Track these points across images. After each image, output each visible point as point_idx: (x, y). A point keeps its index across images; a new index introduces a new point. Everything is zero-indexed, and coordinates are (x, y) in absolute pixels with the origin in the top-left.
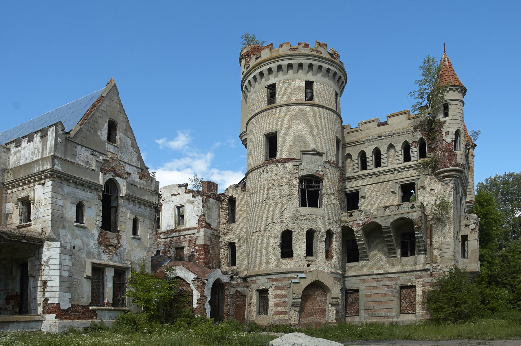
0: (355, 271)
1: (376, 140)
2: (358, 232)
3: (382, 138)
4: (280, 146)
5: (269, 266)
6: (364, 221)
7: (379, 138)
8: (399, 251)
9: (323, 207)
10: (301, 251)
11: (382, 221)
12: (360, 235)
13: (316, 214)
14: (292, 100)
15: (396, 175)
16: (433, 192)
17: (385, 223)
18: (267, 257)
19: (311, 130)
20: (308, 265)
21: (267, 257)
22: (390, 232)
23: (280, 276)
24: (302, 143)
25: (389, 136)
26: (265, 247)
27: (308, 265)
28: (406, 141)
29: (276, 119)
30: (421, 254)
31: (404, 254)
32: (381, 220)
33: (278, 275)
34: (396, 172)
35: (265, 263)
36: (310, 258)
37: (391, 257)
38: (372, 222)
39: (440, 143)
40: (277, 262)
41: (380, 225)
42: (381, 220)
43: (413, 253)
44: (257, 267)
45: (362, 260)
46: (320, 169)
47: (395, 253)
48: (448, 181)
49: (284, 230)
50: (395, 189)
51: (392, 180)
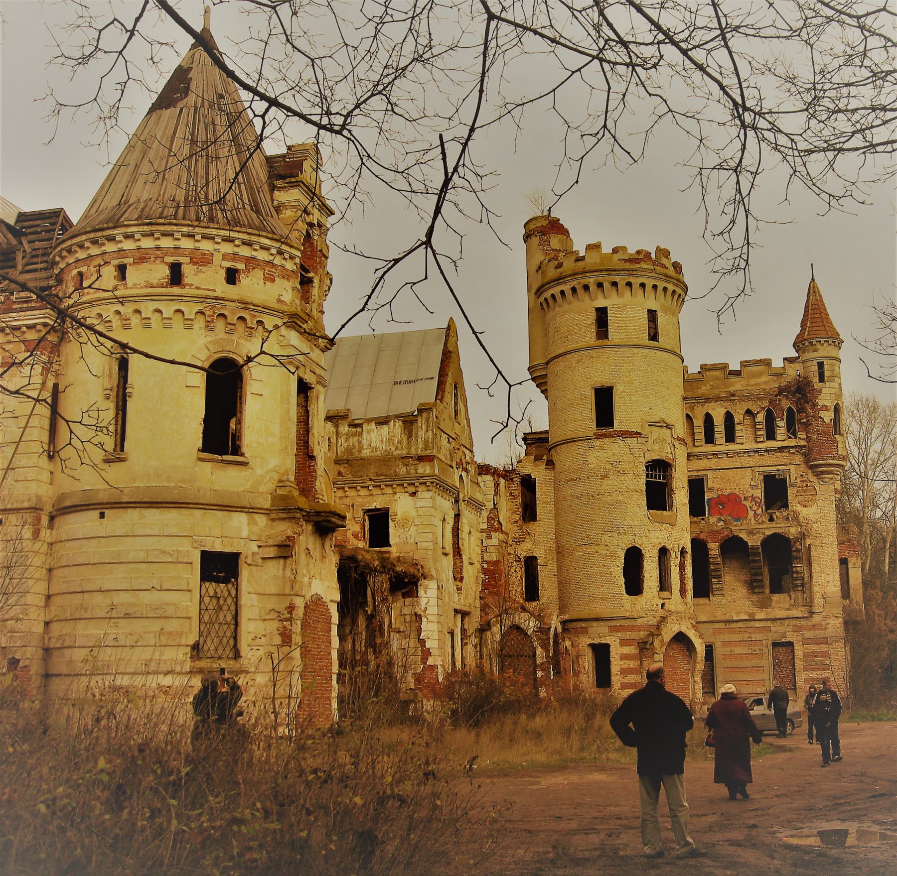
8: (767, 583)
17: (754, 541)
18: (604, 590)
20: (663, 605)
21: (604, 590)
27: (663, 605)
35: (602, 599)
36: (665, 594)
37: (755, 593)
41: (746, 543)
45: (713, 595)
47: (763, 587)
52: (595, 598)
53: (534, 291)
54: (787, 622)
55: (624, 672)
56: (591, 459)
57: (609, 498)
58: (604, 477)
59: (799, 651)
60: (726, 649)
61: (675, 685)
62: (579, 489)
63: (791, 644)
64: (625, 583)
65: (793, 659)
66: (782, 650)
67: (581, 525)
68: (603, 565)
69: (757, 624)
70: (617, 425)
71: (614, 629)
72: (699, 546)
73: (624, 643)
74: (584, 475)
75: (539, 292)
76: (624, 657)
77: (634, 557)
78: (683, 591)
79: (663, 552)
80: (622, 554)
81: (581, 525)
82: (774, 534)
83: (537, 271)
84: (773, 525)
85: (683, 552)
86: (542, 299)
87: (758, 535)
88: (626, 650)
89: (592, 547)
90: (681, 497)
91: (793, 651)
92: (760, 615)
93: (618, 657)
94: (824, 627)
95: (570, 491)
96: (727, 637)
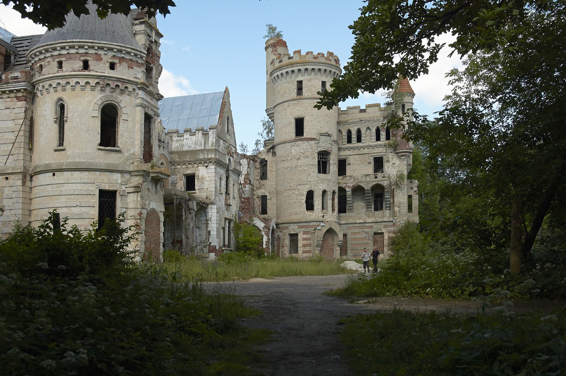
0: (344, 220)
2: (349, 191)
5: (298, 216)
6: (353, 184)
8: (373, 206)
9: (331, 173)
10: (319, 206)
13: (328, 179)
17: (367, 187)
19: (325, 117)
20: (323, 216)
22: (369, 193)
24: (320, 128)
26: (295, 202)
27: (323, 216)
29: (303, 108)
31: (376, 209)
33: (305, 223)
41: (364, 189)
43: (381, 209)
46: (329, 146)
47: (371, 208)
49: (309, 190)
53: (269, 73)
54: (382, 223)
56: (293, 151)
57: (300, 169)
58: (298, 159)
59: (386, 236)
60: (353, 236)
61: (327, 251)
62: (286, 165)
63: (382, 233)
64: (306, 207)
65: (383, 240)
66: (379, 236)
67: (287, 181)
68: (297, 198)
69: (368, 225)
70: (305, 135)
72: (342, 190)
73: (305, 233)
74: (289, 158)
75: (271, 74)
77: (310, 195)
78: (333, 210)
79: (324, 192)
80: (305, 193)
81: (287, 181)
82: (377, 184)
83: (271, 64)
85: (334, 193)
86: (272, 77)
87: (369, 184)
88: (305, 236)
90: (333, 167)
92: (370, 221)
95: (283, 166)
96: (353, 231)
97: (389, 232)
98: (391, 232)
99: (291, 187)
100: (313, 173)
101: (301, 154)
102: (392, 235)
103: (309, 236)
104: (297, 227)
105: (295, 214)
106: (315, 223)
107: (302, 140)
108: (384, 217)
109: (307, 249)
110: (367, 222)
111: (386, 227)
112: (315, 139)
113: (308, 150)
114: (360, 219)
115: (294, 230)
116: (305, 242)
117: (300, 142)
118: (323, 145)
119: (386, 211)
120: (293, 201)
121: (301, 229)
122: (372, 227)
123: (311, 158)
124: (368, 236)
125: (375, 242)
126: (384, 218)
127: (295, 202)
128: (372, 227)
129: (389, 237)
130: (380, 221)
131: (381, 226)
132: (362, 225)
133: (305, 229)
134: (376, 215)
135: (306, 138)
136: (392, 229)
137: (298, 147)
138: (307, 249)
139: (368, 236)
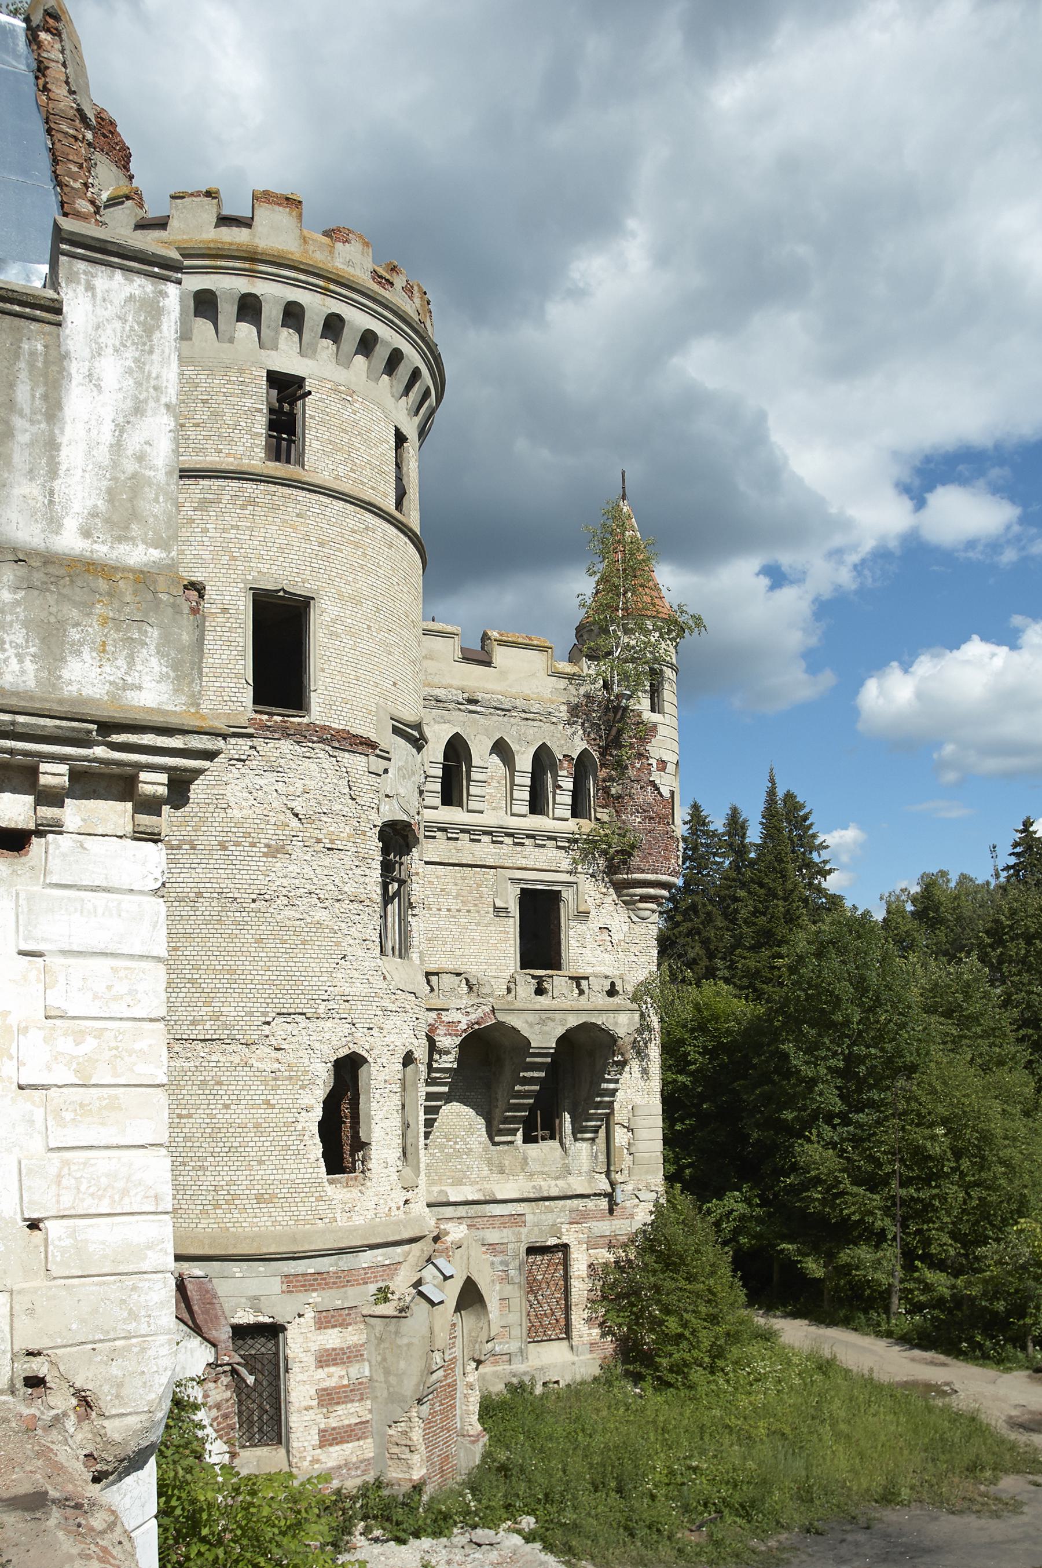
1: (459, 709)
2: (448, 1053)
3: (479, 709)
4: (323, 670)
7: (471, 707)
11: (531, 1025)
12: (449, 1065)
14: (363, 483)
15: (504, 853)
16: (605, 936)
23: (336, 1265)
25: (498, 709)
28: (544, 743)
30: (583, 1140)
32: (527, 1022)
34: (508, 840)
35: (260, 1199)
38: (500, 1026)
39: (641, 788)
40: (317, 1200)
42: (527, 1022)
43: (552, 1132)
44: (204, 1212)
48: (647, 913)
50: (506, 902)
51: (495, 867)
52: (235, 1196)
54: (561, 1203)
55: (328, 1398)
57: (288, 912)
58: (274, 851)
59: (579, 1265)
68: (267, 1102)
71: (295, 1284)
73: (326, 1320)
76: (327, 1359)
84: (583, 1000)
88: (332, 1339)
89: (233, 1047)
91: (566, 1263)
93: (310, 1360)
94: (628, 1212)
97: (591, 1244)
98: (601, 1241)
99: (225, 1026)
100: (360, 953)
101: (294, 822)
102: (605, 1256)
103: (352, 1336)
104: (276, 1285)
105: (260, 1199)
106: (379, 1256)
107: (300, 736)
108: (567, 1171)
109: (347, 1414)
110: (499, 1197)
111: (579, 1218)
112: (372, 745)
113: (337, 807)
114: (460, 1184)
115: (255, 1303)
116: (334, 1376)
117: (286, 746)
118: (402, 791)
119: (579, 1145)
120: (240, 1114)
121: (302, 1297)
122: (517, 1220)
123: (348, 859)
124: (502, 1263)
125: (532, 1287)
126: (571, 1179)
127: (257, 1125)
128: (517, 1220)
129: (591, 1266)
130: (554, 1192)
131: (559, 1212)
132: (473, 1210)
133: (327, 1293)
134: (533, 1166)
135: (324, 728)
136: (605, 1227)
137: (272, 777)
138: (347, 1414)
139: (502, 1263)
